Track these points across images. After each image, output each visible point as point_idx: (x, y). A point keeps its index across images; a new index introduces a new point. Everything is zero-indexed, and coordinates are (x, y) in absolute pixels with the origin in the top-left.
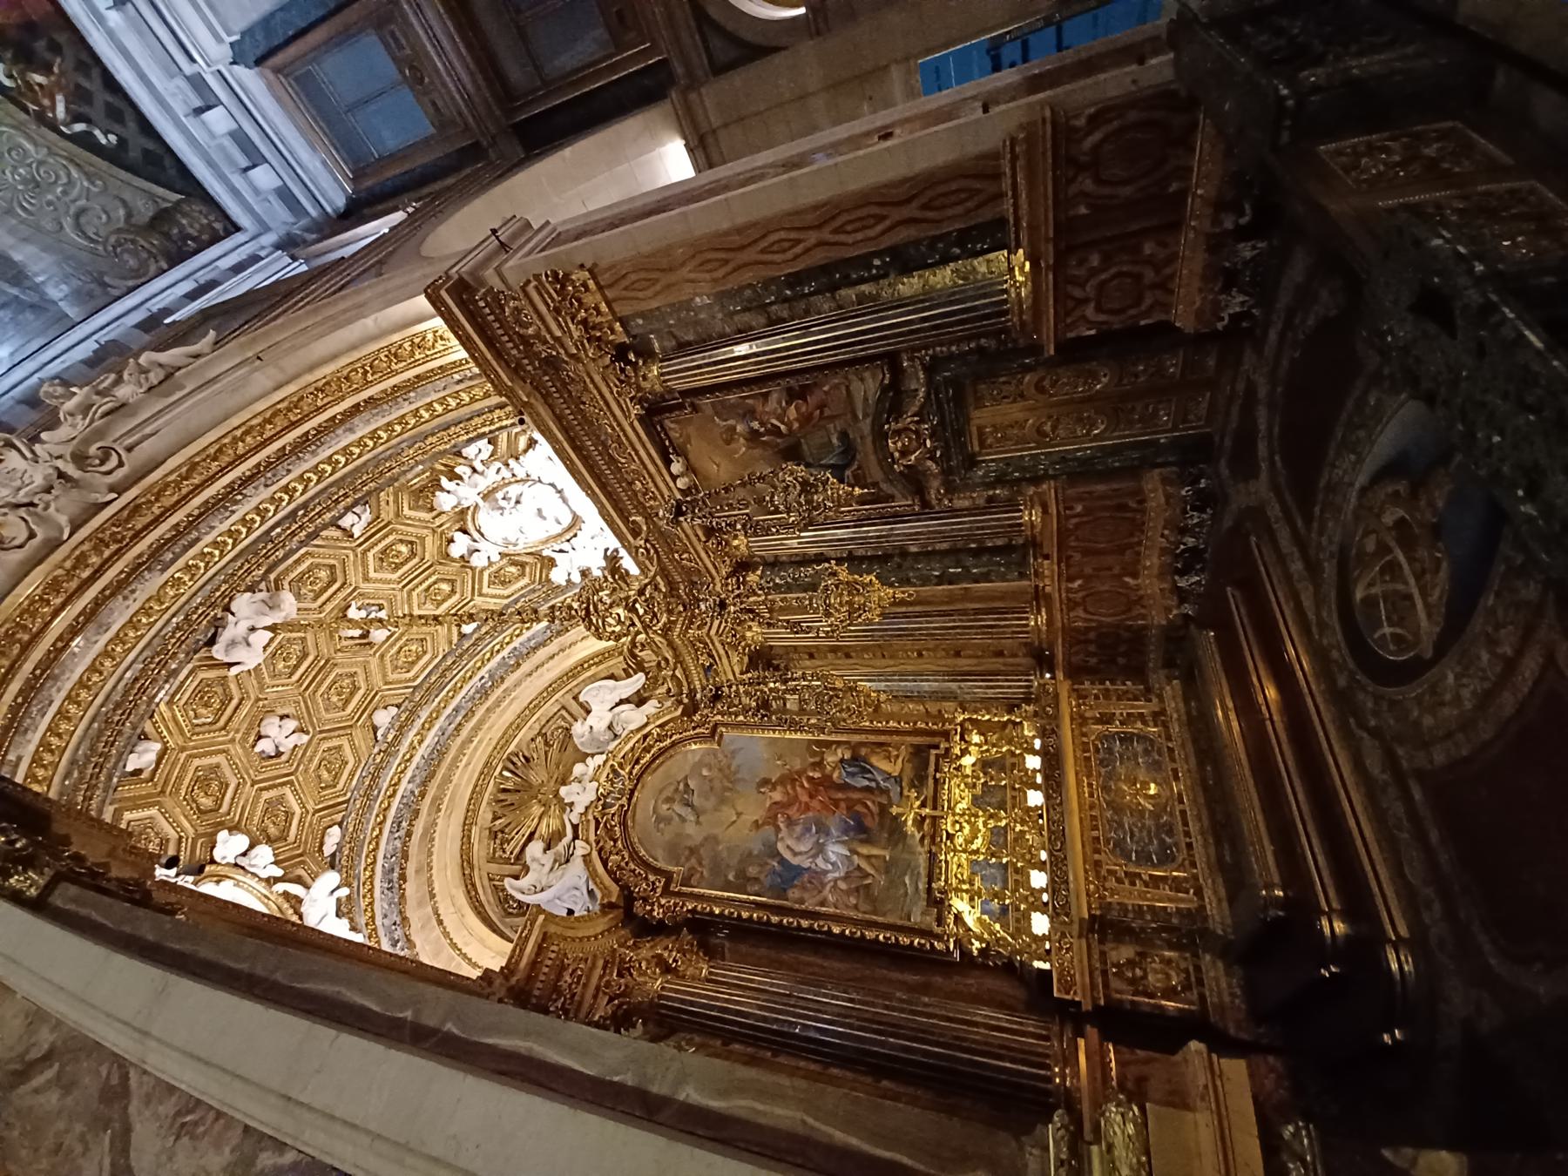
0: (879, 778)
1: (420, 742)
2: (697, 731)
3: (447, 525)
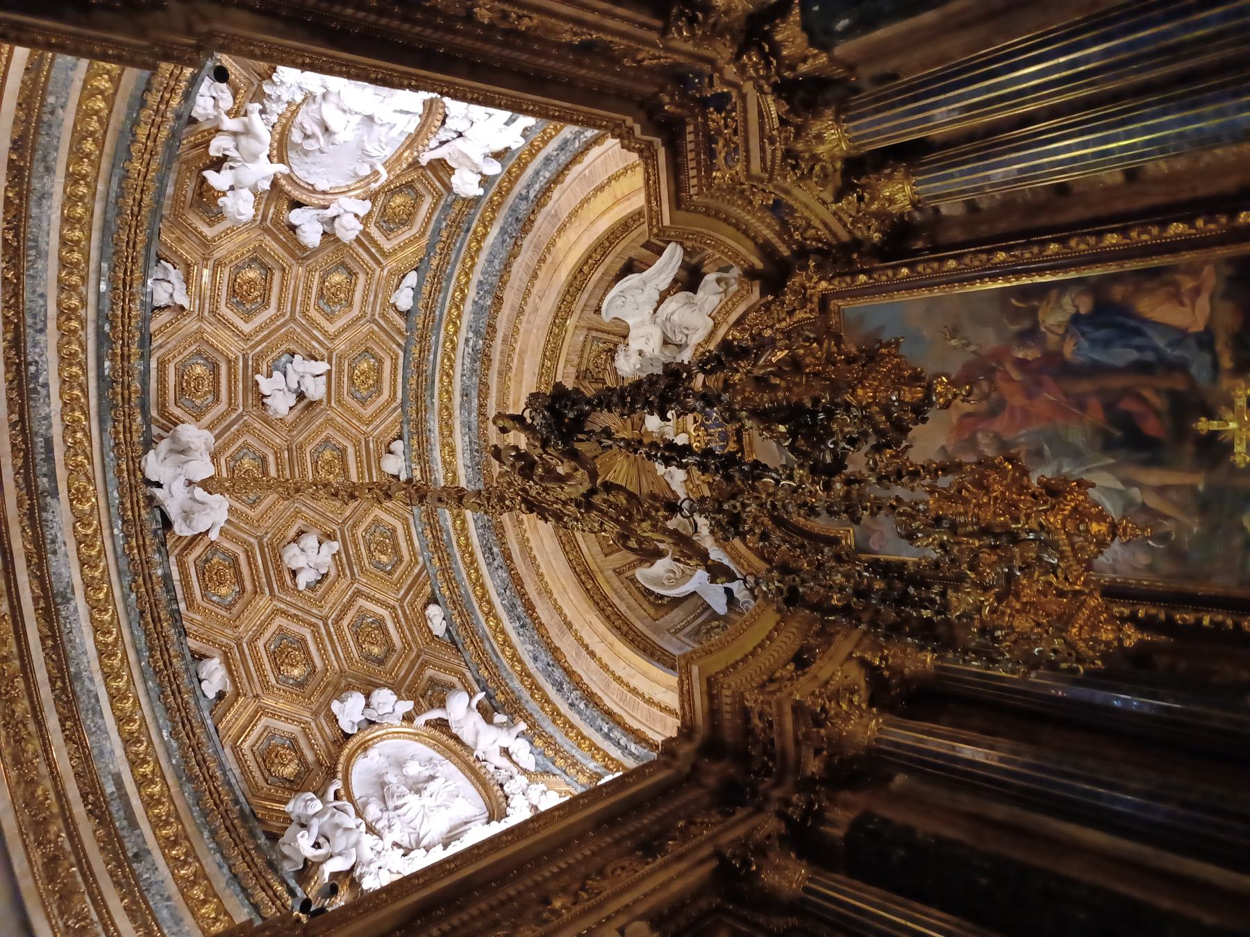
0: (1161, 343)
1: (452, 452)
2: (800, 315)
3: (272, 210)
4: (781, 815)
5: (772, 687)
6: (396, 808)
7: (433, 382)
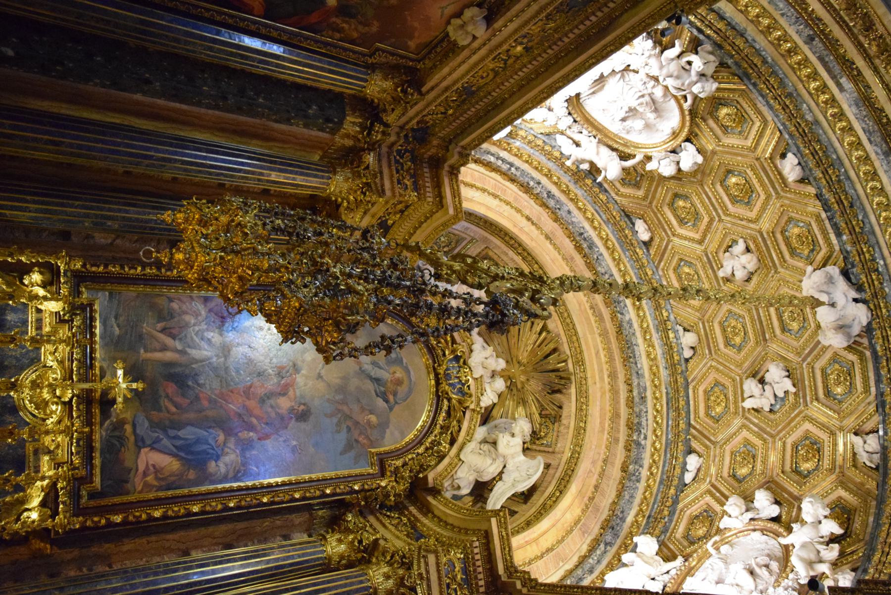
0: (166, 442)
1: (648, 355)
2: (399, 463)
4: (386, 125)
5: (400, 207)
6: (643, 96)
7: (667, 404)
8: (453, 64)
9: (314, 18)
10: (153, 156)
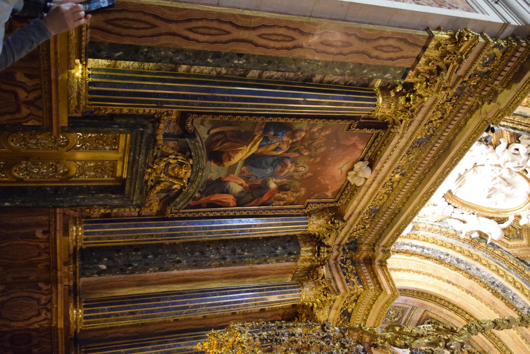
4: (328, 246)
5: (353, 298)
6: (495, 178)
8: (358, 198)
9: (265, 198)
10: (188, 306)
